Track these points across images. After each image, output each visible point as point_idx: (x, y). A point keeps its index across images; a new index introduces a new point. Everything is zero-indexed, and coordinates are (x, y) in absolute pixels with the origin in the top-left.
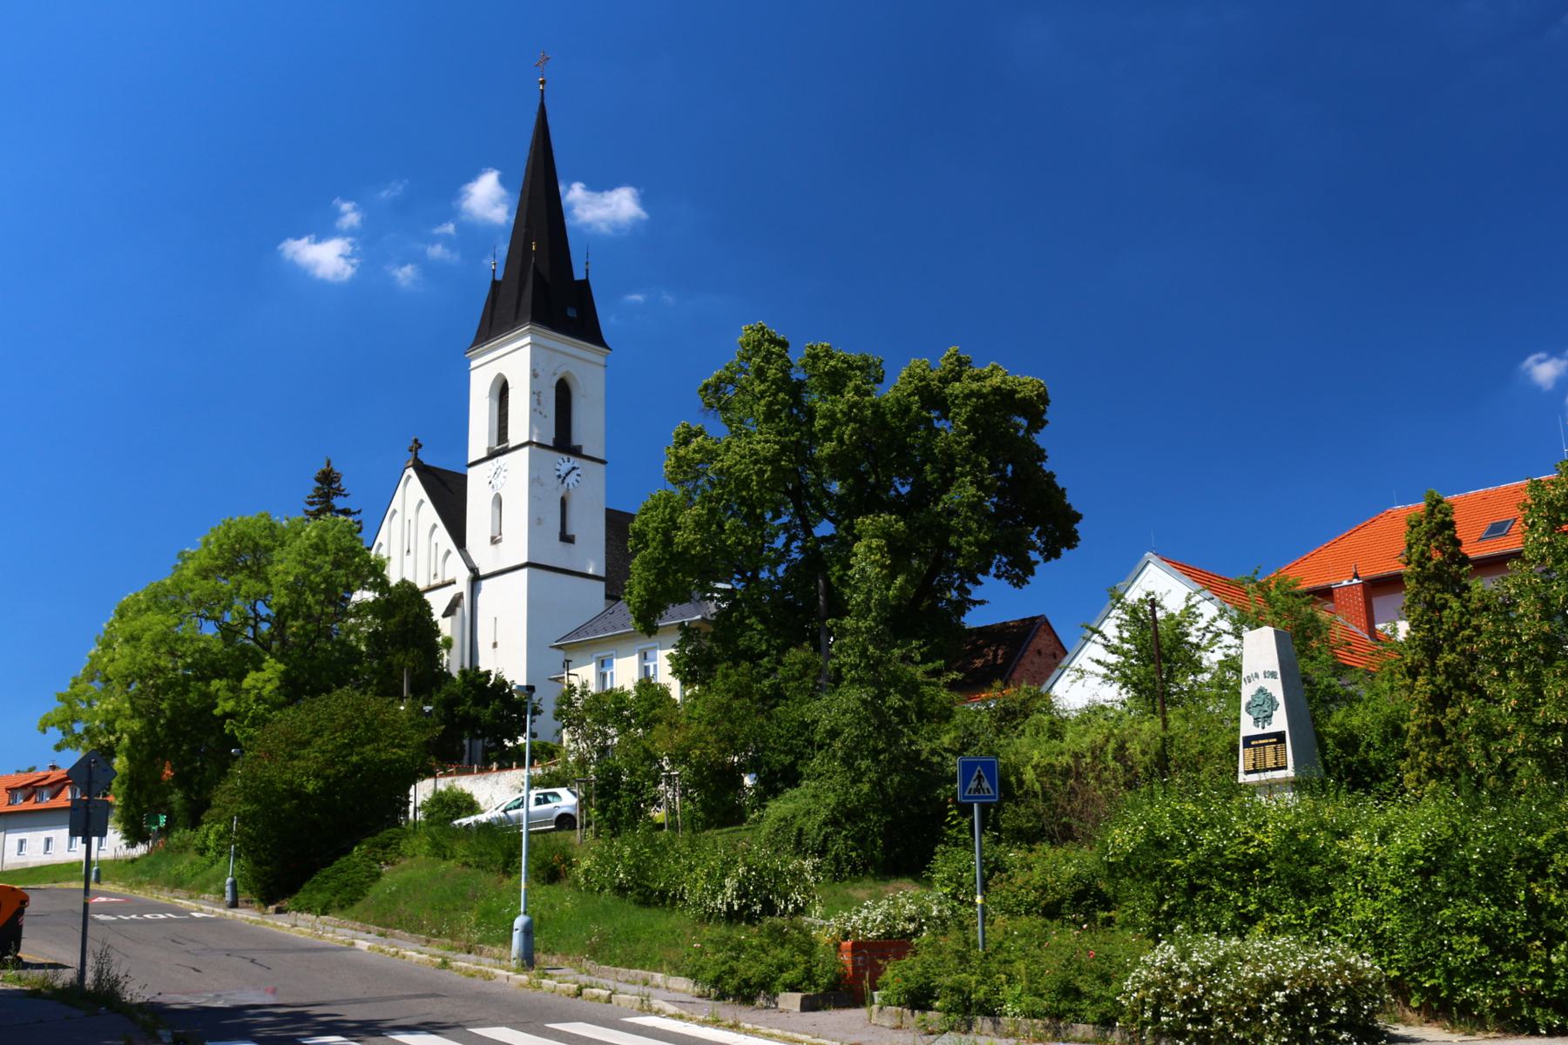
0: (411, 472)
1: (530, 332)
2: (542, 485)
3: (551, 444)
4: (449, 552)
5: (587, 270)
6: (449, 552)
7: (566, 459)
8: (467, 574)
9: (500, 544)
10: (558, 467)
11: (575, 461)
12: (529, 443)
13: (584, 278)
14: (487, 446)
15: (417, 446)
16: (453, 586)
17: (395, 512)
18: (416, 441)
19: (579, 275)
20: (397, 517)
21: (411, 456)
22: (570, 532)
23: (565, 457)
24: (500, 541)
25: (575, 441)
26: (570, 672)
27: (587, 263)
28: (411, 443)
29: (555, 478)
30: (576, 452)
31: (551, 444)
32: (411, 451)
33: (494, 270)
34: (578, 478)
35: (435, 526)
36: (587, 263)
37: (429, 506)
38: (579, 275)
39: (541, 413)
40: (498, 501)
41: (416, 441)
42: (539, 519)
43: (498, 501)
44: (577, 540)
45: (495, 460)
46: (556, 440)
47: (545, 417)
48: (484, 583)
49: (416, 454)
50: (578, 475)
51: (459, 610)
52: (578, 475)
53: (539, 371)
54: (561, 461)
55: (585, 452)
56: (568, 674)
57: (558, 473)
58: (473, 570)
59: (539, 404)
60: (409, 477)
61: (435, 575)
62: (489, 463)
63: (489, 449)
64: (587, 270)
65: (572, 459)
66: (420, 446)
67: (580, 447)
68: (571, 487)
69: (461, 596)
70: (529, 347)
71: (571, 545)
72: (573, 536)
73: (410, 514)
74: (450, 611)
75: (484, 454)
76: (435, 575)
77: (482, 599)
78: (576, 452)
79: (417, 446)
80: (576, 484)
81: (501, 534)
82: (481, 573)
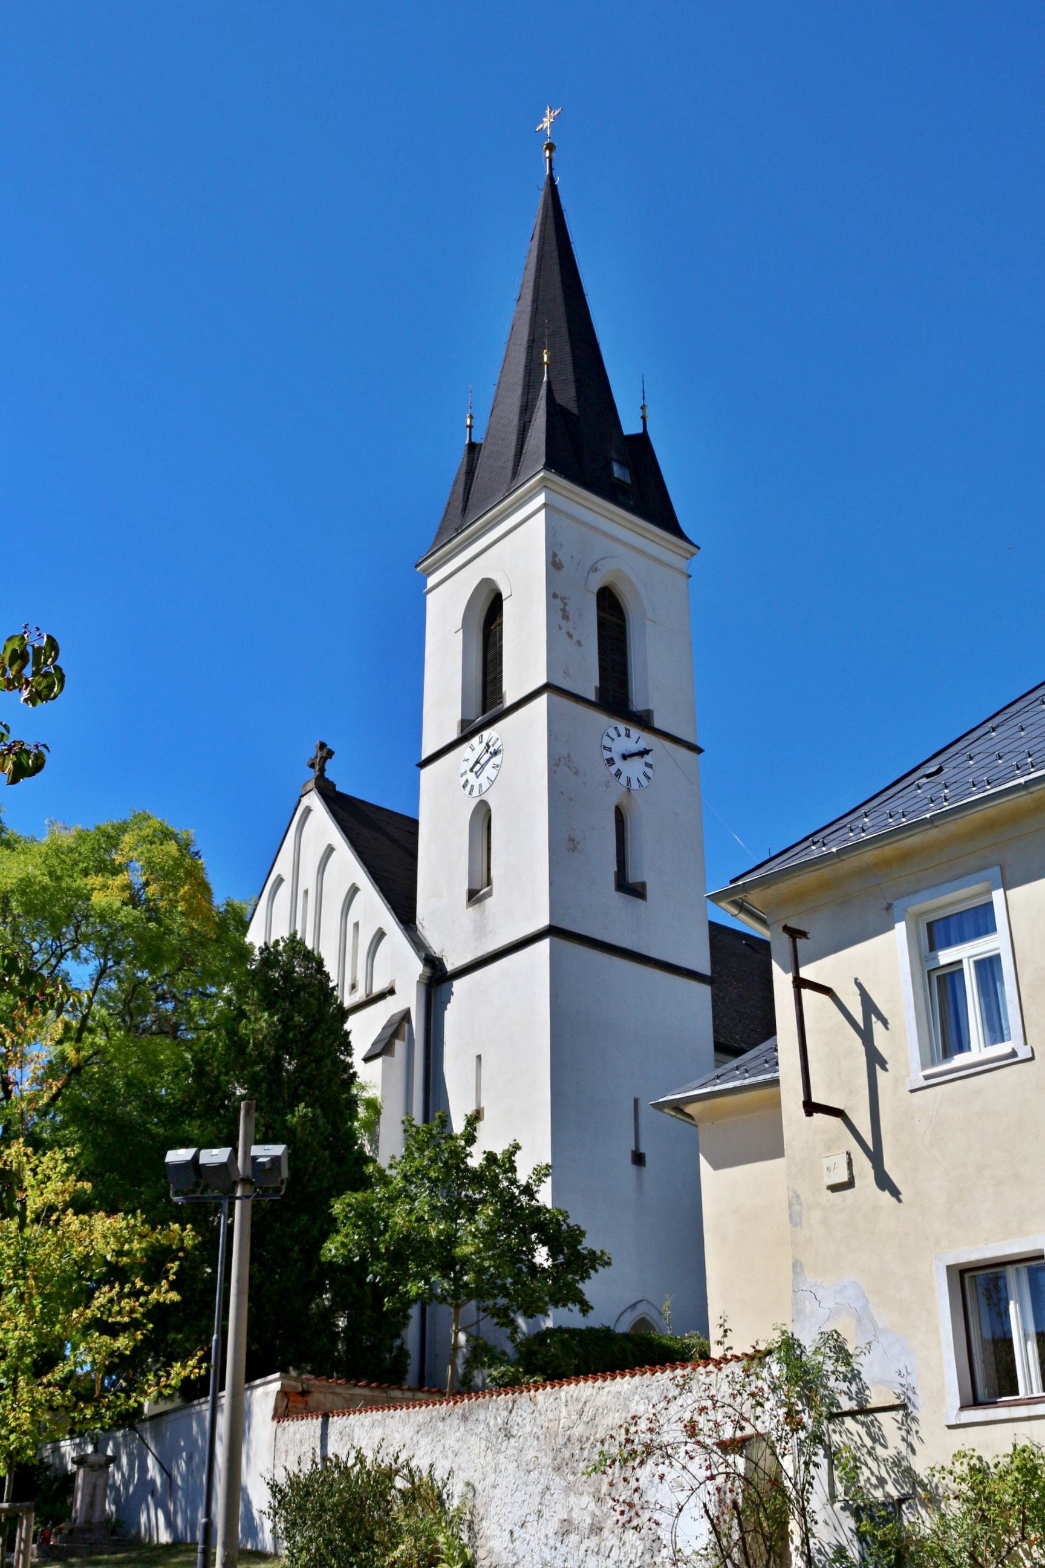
0: (313, 800)
1: (543, 485)
2: (576, 773)
3: (592, 696)
4: (380, 935)
5: (644, 418)
6: (380, 935)
7: (623, 732)
8: (417, 968)
9: (489, 902)
10: (607, 742)
11: (638, 739)
12: (546, 688)
13: (639, 430)
14: (459, 718)
15: (326, 753)
16: (390, 999)
17: (280, 880)
18: (322, 746)
19: (630, 426)
20: (285, 891)
21: (312, 774)
22: (633, 877)
23: (622, 727)
24: (489, 894)
25: (638, 704)
26: (806, 972)
27: (643, 408)
28: (312, 752)
29: (603, 763)
30: (643, 721)
31: (592, 696)
32: (312, 766)
33: (470, 427)
34: (649, 772)
35: (354, 890)
36: (643, 408)
37: (345, 854)
38: (630, 426)
39: (570, 636)
40: (483, 817)
41: (322, 746)
42: (572, 840)
43: (483, 817)
44: (650, 892)
45: (475, 740)
46: (601, 691)
47: (579, 643)
48: (458, 985)
49: (322, 770)
50: (648, 765)
51: (399, 1046)
52: (648, 765)
53: (562, 557)
54: (613, 734)
55: (658, 723)
56: (800, 984)
57: (607, 755)
58: (433, 963)
59: (565, 617)
60: (308, 810)
61: (353, 987)
62: (464, 750)
63: (464, 723)
64: (644, 418)
65: (635, 732)
66: (330, 754)
67: (649, 713)
68: (635, 785)
69: (406, 1016)
70: (542, 514)
71: (639, 901)
72: (643, 885)
73: (308, 880)
74: (382, 1049)
75: (454, 735)
76: (353, 987)
77: (452, 1016)
78: (643, 721)
79: (326, 753)
80: (643, 780)
81: (489, 882)
82: (450, 966)
